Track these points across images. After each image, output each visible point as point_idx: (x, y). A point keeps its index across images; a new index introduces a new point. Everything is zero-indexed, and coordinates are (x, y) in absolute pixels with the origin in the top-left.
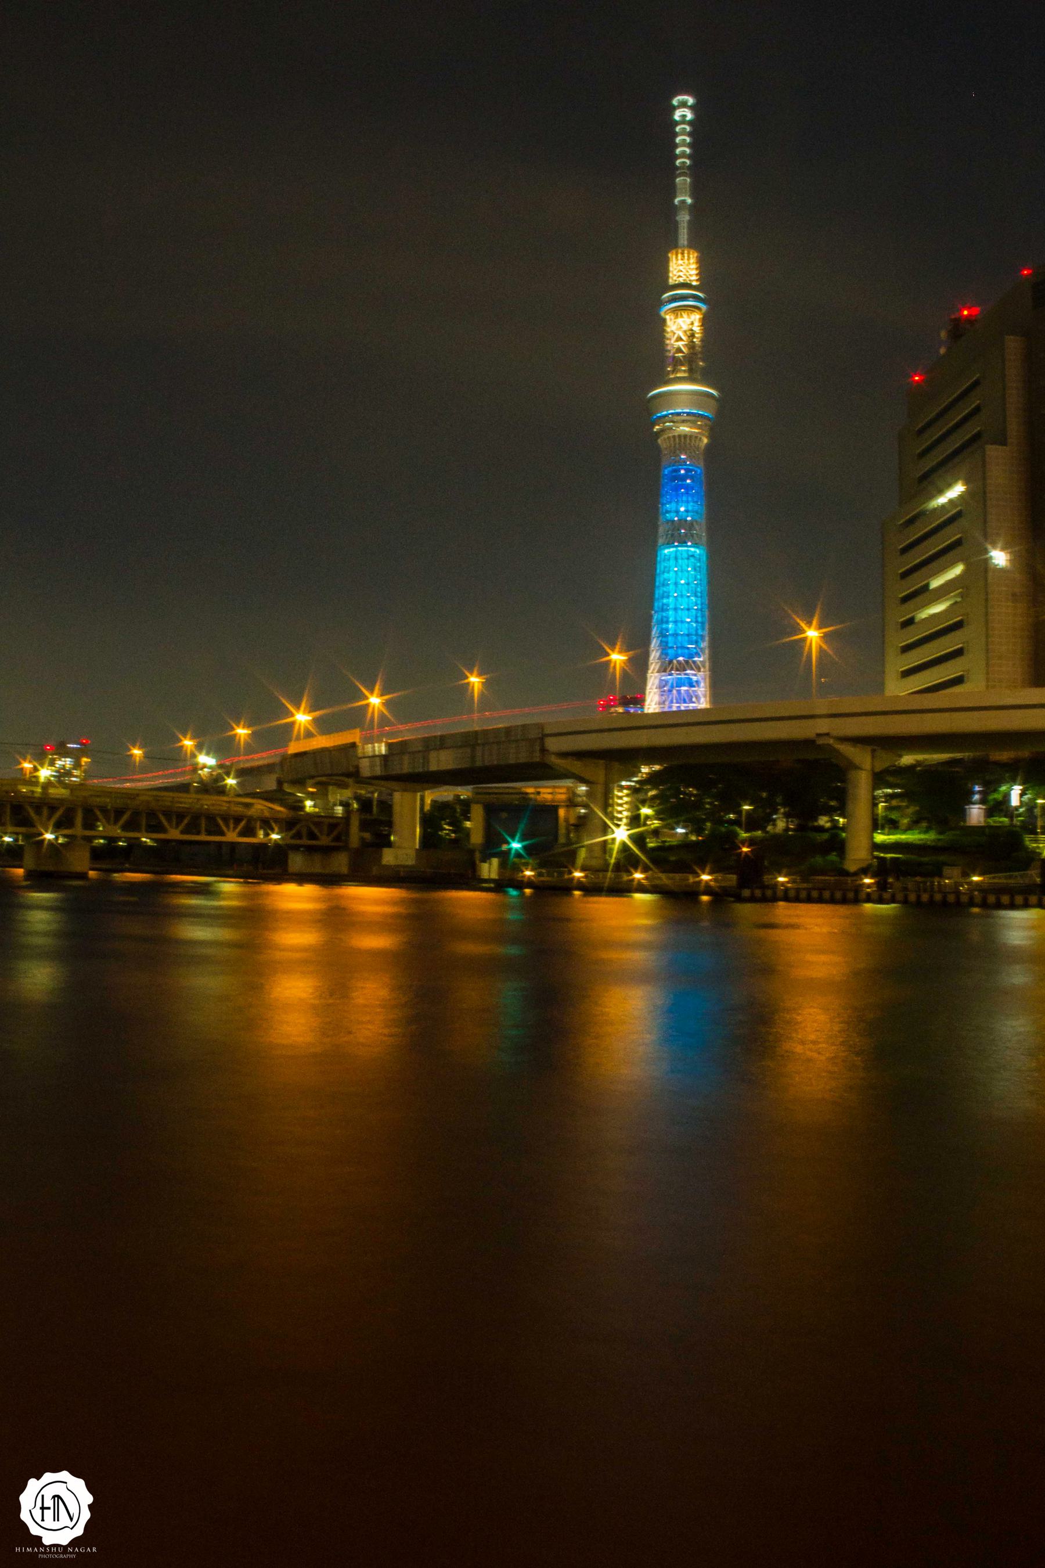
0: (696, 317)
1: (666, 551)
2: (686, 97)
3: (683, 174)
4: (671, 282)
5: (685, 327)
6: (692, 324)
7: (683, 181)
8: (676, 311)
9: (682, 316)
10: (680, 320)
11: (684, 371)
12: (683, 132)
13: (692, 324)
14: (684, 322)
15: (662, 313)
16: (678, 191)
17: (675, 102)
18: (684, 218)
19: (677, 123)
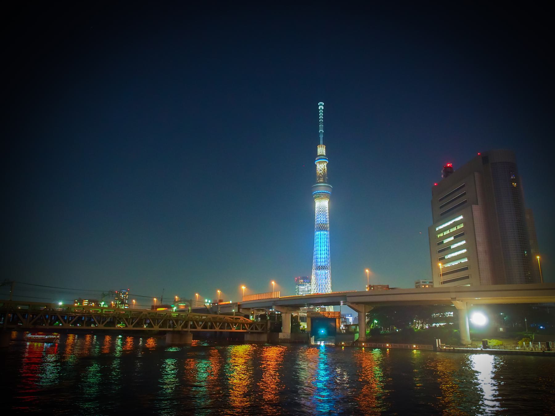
0: (325, 164)
1: (317, 233)
2: (322, 103)
3: (321, 124)
4: (318, 154)
5: (322, 167)
6: (324, 166)
7: (321, 126)
8: (319, 162)
9: (321, 164)
10: (321, 165)
11: (322, 180)
12: (321, 112)
13: (324, 166)
14: (322, 166)
15: (316, 163)
16: (320, 128)
17: (319, 103)
18: (321, 136)
19: (319, 110)
